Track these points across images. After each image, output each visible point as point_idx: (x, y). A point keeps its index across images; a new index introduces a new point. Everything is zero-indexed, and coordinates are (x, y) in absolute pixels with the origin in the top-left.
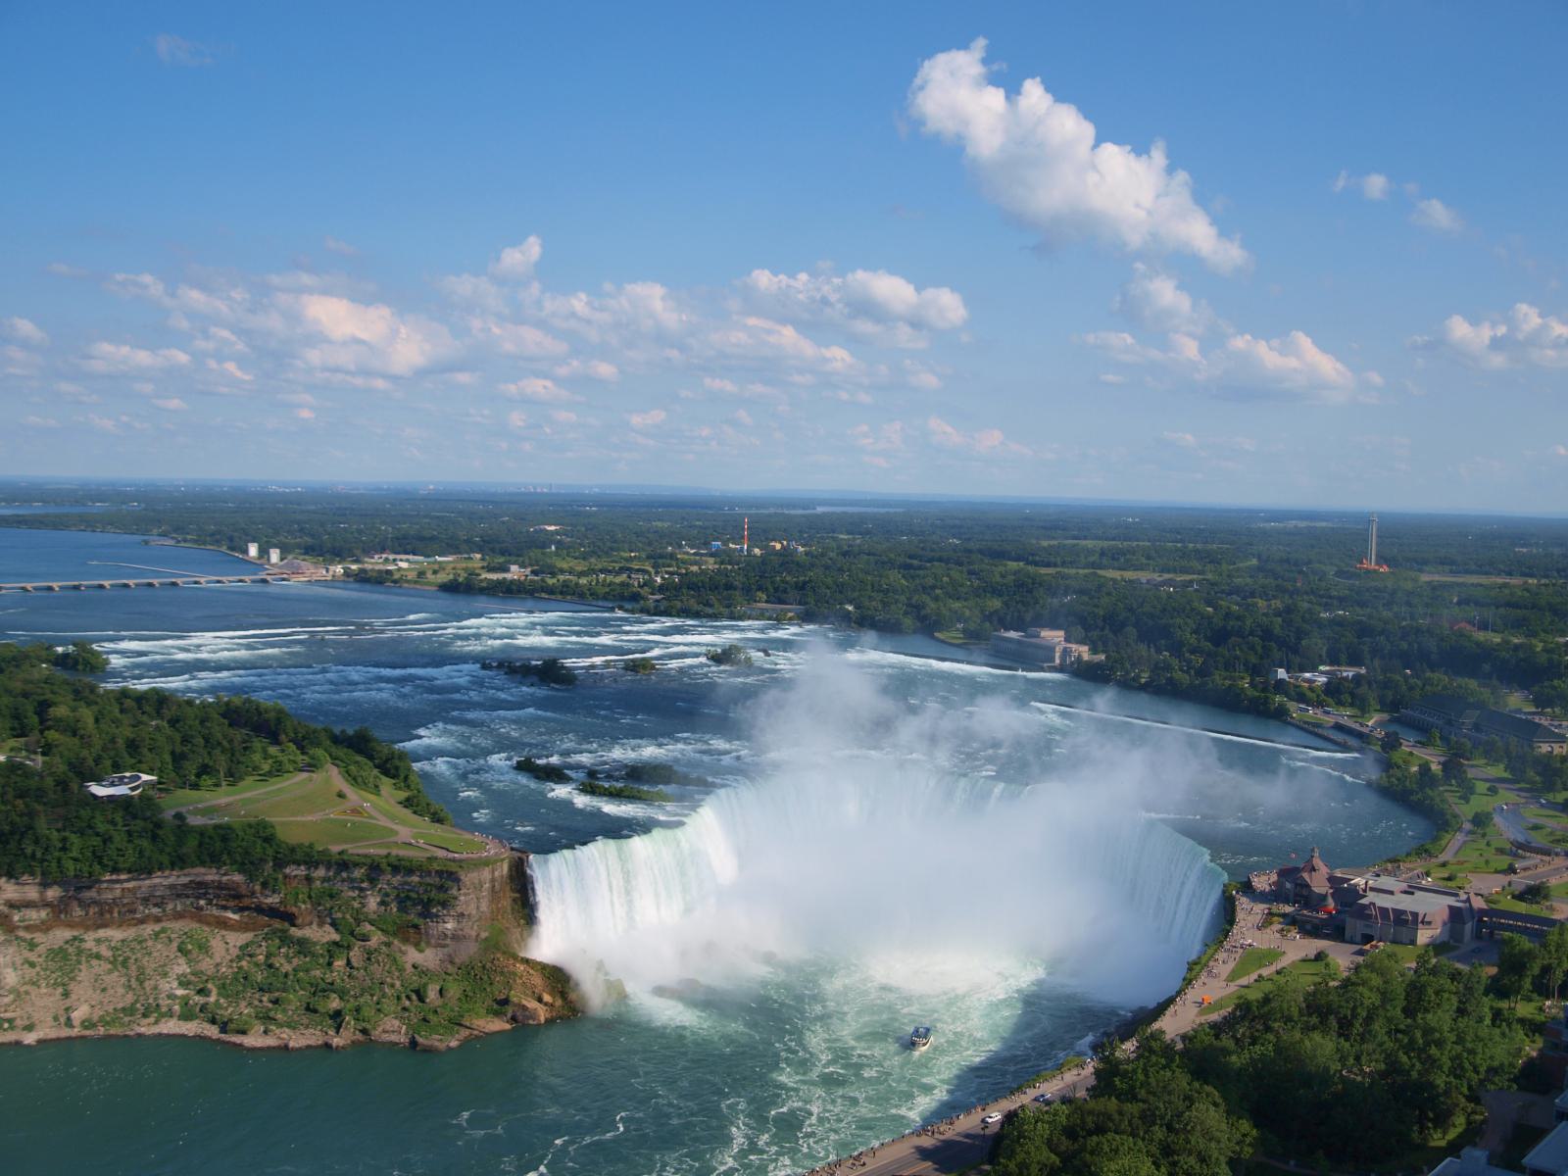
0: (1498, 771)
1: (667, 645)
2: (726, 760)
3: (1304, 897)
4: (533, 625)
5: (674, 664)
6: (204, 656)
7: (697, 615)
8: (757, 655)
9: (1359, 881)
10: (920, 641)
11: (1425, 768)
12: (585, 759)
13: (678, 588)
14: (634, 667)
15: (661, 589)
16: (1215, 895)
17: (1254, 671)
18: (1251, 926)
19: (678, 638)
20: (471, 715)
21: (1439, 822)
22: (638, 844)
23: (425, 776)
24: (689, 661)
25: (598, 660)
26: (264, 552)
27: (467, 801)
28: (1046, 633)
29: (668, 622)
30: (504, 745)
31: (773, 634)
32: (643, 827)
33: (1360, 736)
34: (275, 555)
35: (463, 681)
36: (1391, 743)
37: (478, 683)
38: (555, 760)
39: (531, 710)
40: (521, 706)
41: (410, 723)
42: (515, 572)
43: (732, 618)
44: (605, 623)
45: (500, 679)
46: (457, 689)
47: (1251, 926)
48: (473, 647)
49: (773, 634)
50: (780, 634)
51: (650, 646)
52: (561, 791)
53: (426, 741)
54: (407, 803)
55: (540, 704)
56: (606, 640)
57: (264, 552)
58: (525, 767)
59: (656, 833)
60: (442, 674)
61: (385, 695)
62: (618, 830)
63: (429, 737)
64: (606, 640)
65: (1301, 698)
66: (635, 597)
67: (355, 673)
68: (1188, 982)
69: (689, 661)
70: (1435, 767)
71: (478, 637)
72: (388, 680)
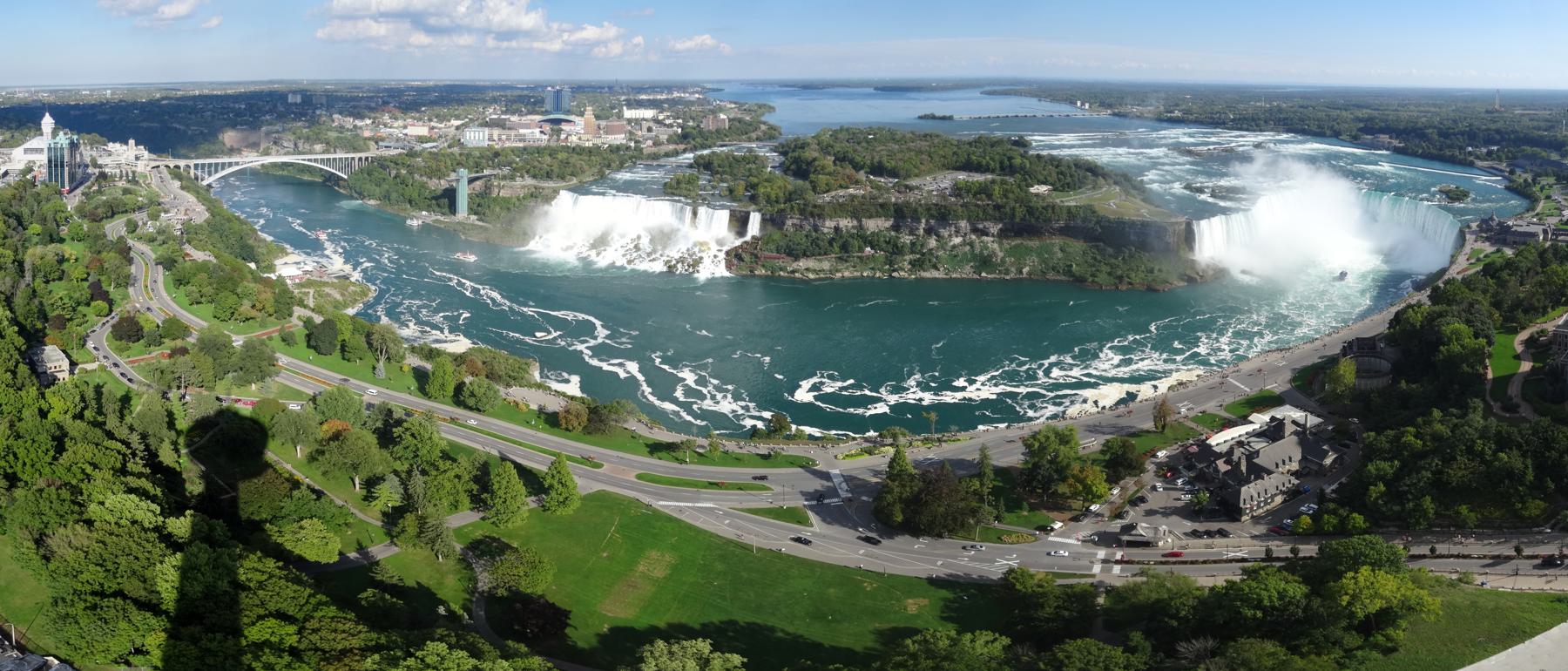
0: (1552, 180)
1: (1237, 142)
2: (1265, 185)
3: (1490, 229)
4: (1185, 134)
5: (1241, 149)
6: (1063, 142)
7: (1247, 130)
8: (1272, 145)
9: (1510, 223)
10: (1334, 140)
11: (1525, 181)
12: (1210, 184)
13: (1239, 119)
14: (1226, 150)
15: (1233, 120)
16: (1456, 231)
17: (1461, 148)
18: (1471, 243)
19: (1240, 139)
20: (1167, 168)
21: (1533, 200)
22: (1234, 216)
23: (1151, 190)
24: (1246, 148)
25: (1211, 147)
26: (1083, 104)
27: (1169, 200)
28: (1382, 136)
29: (1237, 133)
30: (1179, 179)
31: (1277, 137)
32: (1237, 210)
33: (1501, 171)
34: (1087, 106)
35: (1161, 154)
36: (1512, 172)
37: (1166, 156)
38: (1198, 185)
39: (1188, 166)
40: (1184, 164)
41: (1142, 170)
42: (1177, 114)
43: (1261, 131)
44: (1212, 133)
45: (1176, 154)
46: (1159, 158)
47: (1471, 243)
48: (1164, 141)
49: (1277, 137)
50: (1280, 138)
51: (1232, 141)
52: (1203, 197)
53: (1150, 177)
54: (1143, 200)
55: (1192, 164)
56: (1213, 139)
57: (1083, 104)
58: (1188, 187)
59: (1241, 213)
60: (1154, 152)
61: (1133, 160)
62: (1224, 211)
63: (1151, 175)
64: (1213, 139)
65: (1478, 157)
66: (1224, 123)
67: (1121, 150)
68: (1452, 263)
69: (1246, 148)
70: (1530, 180)
71: (1164, 138)
72: (1133, 154)
